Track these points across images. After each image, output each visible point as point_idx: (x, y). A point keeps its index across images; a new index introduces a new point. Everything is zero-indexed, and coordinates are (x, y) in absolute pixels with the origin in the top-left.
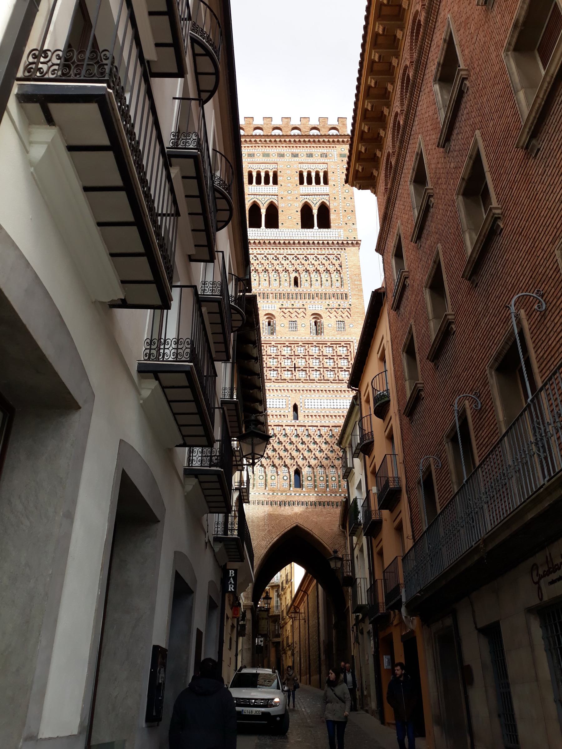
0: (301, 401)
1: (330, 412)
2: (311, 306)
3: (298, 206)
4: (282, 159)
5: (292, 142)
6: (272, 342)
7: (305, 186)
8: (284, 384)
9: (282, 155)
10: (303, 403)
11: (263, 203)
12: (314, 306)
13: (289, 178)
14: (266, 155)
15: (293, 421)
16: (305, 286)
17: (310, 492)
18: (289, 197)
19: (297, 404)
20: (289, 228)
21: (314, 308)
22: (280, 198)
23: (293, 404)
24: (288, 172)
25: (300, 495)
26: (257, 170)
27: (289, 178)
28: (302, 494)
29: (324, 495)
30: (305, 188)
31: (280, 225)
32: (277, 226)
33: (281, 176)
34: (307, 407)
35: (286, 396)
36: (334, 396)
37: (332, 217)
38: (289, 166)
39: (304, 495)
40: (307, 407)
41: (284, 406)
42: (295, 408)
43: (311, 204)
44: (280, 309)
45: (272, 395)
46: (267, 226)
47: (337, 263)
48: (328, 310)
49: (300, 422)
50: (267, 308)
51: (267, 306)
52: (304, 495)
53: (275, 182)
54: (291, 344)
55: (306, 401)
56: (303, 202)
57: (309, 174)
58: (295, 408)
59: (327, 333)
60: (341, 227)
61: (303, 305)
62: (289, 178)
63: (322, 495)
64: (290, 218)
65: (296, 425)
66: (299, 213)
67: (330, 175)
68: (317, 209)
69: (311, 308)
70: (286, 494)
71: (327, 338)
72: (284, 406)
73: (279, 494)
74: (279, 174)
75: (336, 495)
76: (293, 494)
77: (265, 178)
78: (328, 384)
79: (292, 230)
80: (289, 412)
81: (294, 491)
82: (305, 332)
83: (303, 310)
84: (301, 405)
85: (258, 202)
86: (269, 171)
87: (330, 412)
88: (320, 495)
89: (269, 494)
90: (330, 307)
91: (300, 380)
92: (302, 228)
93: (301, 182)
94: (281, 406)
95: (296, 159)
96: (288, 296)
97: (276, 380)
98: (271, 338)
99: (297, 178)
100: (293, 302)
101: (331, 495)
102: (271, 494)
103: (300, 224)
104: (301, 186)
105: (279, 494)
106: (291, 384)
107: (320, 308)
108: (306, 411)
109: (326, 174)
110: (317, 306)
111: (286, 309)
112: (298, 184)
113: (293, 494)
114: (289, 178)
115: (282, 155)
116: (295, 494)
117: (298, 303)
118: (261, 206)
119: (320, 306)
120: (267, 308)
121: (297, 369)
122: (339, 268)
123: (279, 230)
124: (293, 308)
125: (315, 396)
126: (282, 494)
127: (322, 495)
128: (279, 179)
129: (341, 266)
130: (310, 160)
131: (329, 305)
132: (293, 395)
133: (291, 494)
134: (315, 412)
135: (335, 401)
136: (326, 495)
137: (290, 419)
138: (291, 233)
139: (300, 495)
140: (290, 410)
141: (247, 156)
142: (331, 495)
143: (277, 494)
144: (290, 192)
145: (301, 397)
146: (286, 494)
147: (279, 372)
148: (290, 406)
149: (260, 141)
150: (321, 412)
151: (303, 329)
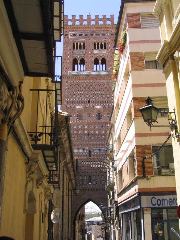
7: (96, 50)
13: (89, 45)
26: (77, 42)
30: (96, 51)
41: (85, 151)
42: (90, 151)
54: (89, 124)
56: (95, 58)
57: (98, 44)
58: (90, 151)
67: (106, 44)
72: (85, 151)
77: (79, 45)
93: (95, 48)
95: (92, 37)
99: (93, 46)
109: (105, 44)
114: (89, 45)
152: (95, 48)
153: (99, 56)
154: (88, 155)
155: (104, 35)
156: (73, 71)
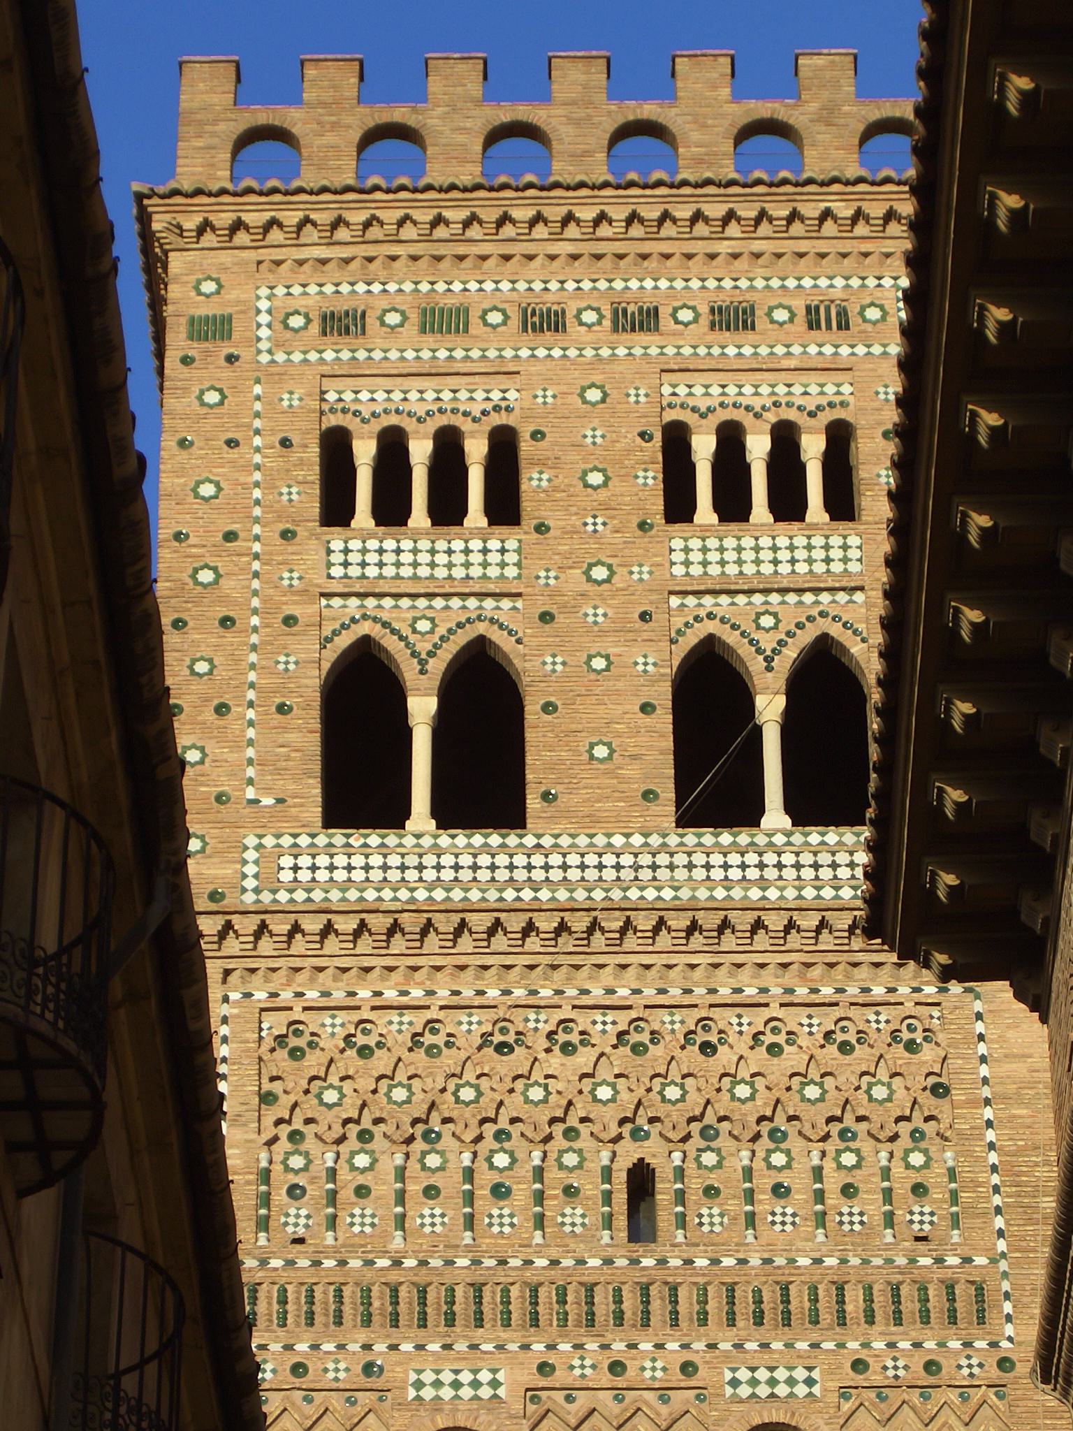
2: (743, 1375)
3: (653, 667)
4: (547, 349)
9: (545, 322)
11: (423, 647)
12: (763, 1374)
14: (443, 320)
16: (702, 1241)
18: (596, 613)
20: (592, 822)
21: (763, 1391)
24: (593, 434)
27: (595, 478)
31: (533, 802)
33: (542, 464)
38: (594, 395)
43: (745, 651)
46: (449, 814)
50: (447, 1393)
51: (447, 1377)
53: (504, 508)
56: (691, 639)
62: (595, 478)
64: (601, 752)
66: (664, 720)
68: (781, 684)
69: (744, 1391)
74: (526, 447)
79: (618, 841)
85: (391, 644)
86: (466, 426)
90: (875, 1377)
92: (686, 819)
93: (679, 507)
95: (643, 344)
96: (585, 1307)
99: (650, 479)
103: (668, 793)
104: (677, 537)
107: (801, 1390)
110: (781, 1374)
112: (659, 519)
115: (545, 322)
117: (654, 1356)
118: (409, 671)
119: (800, 1374)
120: (447, 1393)
123: (530, 841)
128: (532, 481)
130: (736, 347)
138: (609, 860)
141: (315, 328)
144: (600, 573)
152: (679, 507)
153: (748, 626)
156: (338, 836)
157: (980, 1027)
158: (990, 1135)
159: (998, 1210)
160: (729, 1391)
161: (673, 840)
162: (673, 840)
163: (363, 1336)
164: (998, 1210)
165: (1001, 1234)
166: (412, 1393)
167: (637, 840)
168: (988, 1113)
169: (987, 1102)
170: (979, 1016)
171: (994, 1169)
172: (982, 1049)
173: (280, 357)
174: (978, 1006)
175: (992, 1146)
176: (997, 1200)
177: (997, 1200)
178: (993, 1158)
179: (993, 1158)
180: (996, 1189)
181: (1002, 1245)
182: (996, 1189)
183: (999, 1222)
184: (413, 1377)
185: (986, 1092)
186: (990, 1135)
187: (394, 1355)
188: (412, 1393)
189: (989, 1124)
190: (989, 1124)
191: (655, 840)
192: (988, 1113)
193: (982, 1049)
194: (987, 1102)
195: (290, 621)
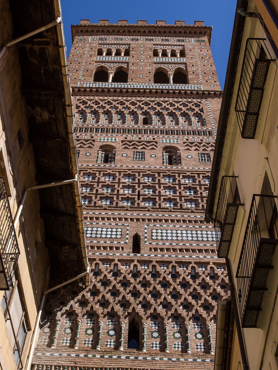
0: (146, 231)
1: (191, 245)
5: (147, 32)
6: (108, 170)
8: (121, 212)
10: (150, 234)
15: (132, 255)
17: (157, 354)
19: (140, 234)
22: (130, 65)
23: (133, 233)
25: (136, 358)
28: (140, 358)
29: (182, 360)
32: (125, 81)
33: (133, 51)
34: (154, 238)
35: (123, 225)
36: (197, 227)
37: (190, 77)
39: (145, 358)
40: (154, 238)
44: (122, 141)
45: (101, 224)
47: (197, 109)
48: (186, 144)
49: (142, 255)
52: (145, 358)
55: (154, 231)
59: (186, 164)
60: (200, 84)
61: (154, 139)
63: (178, 359)
65: (136, 259)
70: (111, 357)
71: (185, 168)
72: (119, 237)
73: (98, 356)
75: (204, 361)
76: (123, 357)
78: (189, 214)
80: (126, 243)
81: (125, 352)
82: (155, 160)
83: (154, 143)
84: (146, 235)
87: (191, 245)
88: (173, 359)
89: (77, 355)
91: (146, 208)
94: (114, 236)
97: (109, 207)
98: (107, 166)
100: (140, 136)
101: (195, 360)
102: (82, 355)
103: (152, 80)
105: (98, 356)
106: (131, 212)
108: (154, 244)
111: (130, 142)
113: (123, 357)
116: (128, 358)
121: (141, 197)
122: (199, 112)
123: (128, 84)
124: (140, 142)
125: (168, 226)
126: (102, 357)
127: (178, 359)
129: (202, 110)
131: (187, 140)
132: (134, 223)
133: (119, 357)
134: (167, 244)
135: (199, 232)
136: (185, 360)
137: (127, 253)
139: (136, 358)
140: (127, 241)
142: (195, 360)
143: (94, 356)
145: (146, 226)
146: (111, 357)
147: (115, 199)
148: (127, 236)
149: (113, 31)
150: (177, 244)
151: (152, 159)
154: (129, 249)
155: (179, 41)
157: (208, 104)
158: (211, 115)
159: (213, 123)
160: (161, 142)
161: (153, 84)
162: (153, 84)
163: (90, 133)
164: (213, 123)
165: (214, 126)
166: (99, 140)
167: (147, 84)
168: (210, 113)
169: (210, 112)
170: (208, 103)
171: (212, 119)
172: (209, 106)
173: (92, 42)
174: (208, 102)
175: (211, 116)
176: (213, 122)
177: (213, 122)
178: (212, 118)
179: (212, 118)
180: (212, 121)
181: (214, 127)
182: (212, 121)
183: (213, 124)
184: (99, 138)
185: (210, 111)
186: (211, 115)
187: (96, 136)
188: (99, 140)
189: (211, 114)
190: (211, 114)
191: (150, 84)
192: (210, 113)
193: (209, 106)
194: (210, 112)
195: (90, 63)
